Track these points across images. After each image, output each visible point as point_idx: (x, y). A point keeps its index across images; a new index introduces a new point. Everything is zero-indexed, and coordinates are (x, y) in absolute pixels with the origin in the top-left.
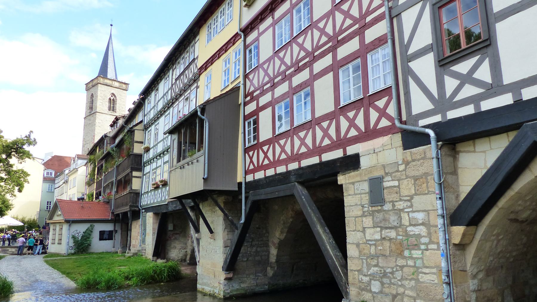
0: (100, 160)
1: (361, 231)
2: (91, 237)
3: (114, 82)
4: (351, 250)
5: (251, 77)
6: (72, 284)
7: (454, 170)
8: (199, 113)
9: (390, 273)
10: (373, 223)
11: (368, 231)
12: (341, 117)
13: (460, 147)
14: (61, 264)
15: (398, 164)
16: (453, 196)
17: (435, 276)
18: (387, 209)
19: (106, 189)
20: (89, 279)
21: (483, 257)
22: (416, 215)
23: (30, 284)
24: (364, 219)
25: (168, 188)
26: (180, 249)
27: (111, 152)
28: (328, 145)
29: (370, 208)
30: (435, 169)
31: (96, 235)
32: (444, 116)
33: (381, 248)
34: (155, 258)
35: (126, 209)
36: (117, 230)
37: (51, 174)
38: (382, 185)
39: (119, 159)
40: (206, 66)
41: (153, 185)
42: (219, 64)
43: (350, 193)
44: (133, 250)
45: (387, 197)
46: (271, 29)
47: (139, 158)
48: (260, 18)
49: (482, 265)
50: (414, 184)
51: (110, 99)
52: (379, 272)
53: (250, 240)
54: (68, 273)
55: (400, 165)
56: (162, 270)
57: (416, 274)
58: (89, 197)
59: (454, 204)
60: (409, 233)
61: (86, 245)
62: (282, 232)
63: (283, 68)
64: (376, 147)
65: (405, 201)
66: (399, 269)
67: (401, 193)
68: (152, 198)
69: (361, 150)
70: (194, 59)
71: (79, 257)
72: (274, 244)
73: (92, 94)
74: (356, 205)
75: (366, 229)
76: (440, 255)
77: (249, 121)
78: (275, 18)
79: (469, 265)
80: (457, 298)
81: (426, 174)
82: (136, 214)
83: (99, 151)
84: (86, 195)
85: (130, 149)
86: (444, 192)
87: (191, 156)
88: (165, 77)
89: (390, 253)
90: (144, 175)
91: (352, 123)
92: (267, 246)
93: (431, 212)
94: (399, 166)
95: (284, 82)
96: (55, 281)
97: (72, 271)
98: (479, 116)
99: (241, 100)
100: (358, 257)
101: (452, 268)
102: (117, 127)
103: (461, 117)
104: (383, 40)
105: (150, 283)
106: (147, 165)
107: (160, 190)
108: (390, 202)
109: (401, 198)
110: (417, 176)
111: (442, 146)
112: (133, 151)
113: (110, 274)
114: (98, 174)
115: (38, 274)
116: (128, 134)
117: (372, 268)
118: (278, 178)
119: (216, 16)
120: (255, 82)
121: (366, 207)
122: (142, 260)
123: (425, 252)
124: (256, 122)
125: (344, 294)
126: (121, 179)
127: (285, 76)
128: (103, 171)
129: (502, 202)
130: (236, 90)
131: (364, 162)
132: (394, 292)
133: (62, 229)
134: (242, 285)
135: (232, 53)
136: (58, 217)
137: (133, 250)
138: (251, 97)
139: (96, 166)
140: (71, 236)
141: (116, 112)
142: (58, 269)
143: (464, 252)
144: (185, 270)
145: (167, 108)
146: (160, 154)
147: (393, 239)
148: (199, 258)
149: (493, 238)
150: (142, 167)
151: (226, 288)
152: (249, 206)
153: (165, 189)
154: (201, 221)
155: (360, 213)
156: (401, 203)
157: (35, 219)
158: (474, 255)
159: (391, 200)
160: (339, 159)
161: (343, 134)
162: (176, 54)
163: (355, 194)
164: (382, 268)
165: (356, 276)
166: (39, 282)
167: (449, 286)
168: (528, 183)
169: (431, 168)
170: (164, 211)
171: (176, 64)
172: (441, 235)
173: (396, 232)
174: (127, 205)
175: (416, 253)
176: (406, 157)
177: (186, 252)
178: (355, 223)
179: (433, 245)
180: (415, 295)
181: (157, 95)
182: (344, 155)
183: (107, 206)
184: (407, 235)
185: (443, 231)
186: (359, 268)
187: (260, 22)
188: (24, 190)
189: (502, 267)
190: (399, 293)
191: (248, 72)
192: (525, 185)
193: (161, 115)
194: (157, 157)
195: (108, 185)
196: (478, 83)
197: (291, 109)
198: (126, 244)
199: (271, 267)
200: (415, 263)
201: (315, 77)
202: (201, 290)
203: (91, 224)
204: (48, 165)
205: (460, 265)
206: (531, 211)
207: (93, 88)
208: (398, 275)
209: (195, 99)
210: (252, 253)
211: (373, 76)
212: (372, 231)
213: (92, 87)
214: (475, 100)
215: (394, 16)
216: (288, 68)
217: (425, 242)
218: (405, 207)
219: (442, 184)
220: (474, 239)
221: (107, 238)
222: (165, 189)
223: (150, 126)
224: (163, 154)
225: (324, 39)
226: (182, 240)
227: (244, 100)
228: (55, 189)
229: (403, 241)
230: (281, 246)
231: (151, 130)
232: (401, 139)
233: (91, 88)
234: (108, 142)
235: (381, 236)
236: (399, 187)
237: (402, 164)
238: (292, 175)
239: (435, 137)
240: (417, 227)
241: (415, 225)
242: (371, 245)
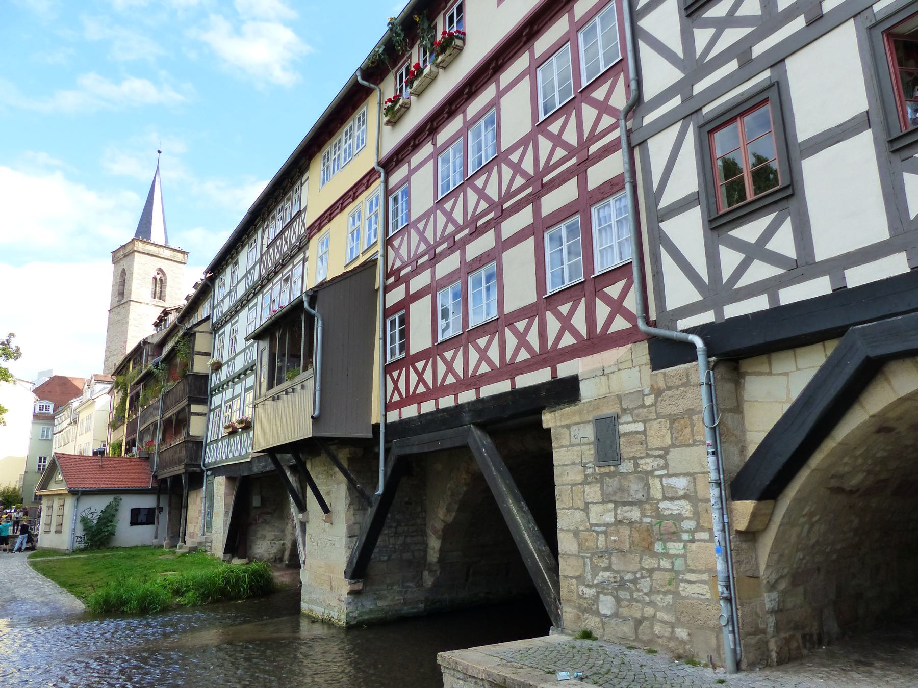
0: (134, 385)
1: (582, 510)
2: (116, 519)
4: (566, 543)
5: (396, 243)
6: (79, 606)
7: (736, 404)
8: (306, 305)
9: (631, 581)
10: (602, 495)
11: (593, 509)
12: (549, 314)
13: (746, 365)
15: (643, 394)
16: (735, 448)
17: (707, 587)
18: (624, 471)
19: (144, 436)
20: (108, 595)
21: (787, 552)
22: (673, 481)
24: (587, 488)
25: (252, 432)
26: (273, 540)
27: (154, 370)
28: (525, 361)
29: (597, 468)
30: (705, 404)
31: (124, 516)
32: (719, 313)
33: (616, 538)
34: (228, 556)
35: (179, 469)
36: (162, 508)
37: (48, 408)
38: (617, 430)
39: (168, 382)
41: (227, 427)
42: (342, 220)
43: (563, 444)
44: (190, 542)
45: (626, 449)
46: (431, 163)
47: (203, 381)
48: (412, 144)
49: (785, 568)
50: (671, 428)
51: (155, 278)
52: (612, 580)
53: (394, 525)
54: (72, 585)
55: (646, 395)
56: (240, 578)
57: (674, 583)
58: (114, 449)
59: (737, 462)
60: (662, 513)
61: (106, 534)
62: (448, 510)
63: (451, 228)
64: (606, 365)
65: (656, 457)
66: (646, 575)
67: (649, 444)
68: (225, 451)
69: (581, 370)
70: (300, 211)
72: (435, 532)
73: (124, 269)
74: (574, 463)
75: (589, 505)
76: (714, 551)
77: (392, 318)
78: (438, 145)
79: (763, 567)
80: (743, 624)
81: (690, 412)
82: (196, 479)
83: (134, 368)
84: (108, 446)
85: (186, 365)
86: (720, 443)
87: (291, 378)
88: (250, 243)
89: (630, 547)
90: (210, 410)
91: (566, 324)
92: (424, 534)
93: (700, 478)
94: (645, 398)
95: (453, 252)
96: (47, 599)
97: (79, 581)
98: (777, 313)
99: (379, 282)
100: (577, 553)
101: (735, 573)
103: (746, 316)
104: (617, 184)
105: (218, 601)
106: (216, 394)
107: (238, 437)
108: (630, 459)
109: (649, 452)
110: (675, 414)
111: (716, 364)
112: (192, 369)
113: (147, 585)
114: (130, 409)
115: (17, 587)
116: (183, 339)
117: (601, 574)
118: (441, 416)
119: (339, 138)
120: (404, 252)
121: (590, 468)
122: (205, 559)
123: (689, 544)
124: (404, 321)
125: (552, 619)
127: (454, 242)
128: (140, 403)
129: (817, 459)
130: (371, 264)
131: (586, 390)
132: (638, 615)
133: (63, 505)
134: (380, 604)
135: (364, 203)
136: (58, 486)
137: (190, 542)
138: (396, 277)
139: (127, 396)
140: (79, 519)
141: (164, 301)
142: (54, 578)
143: (755, 546)
144: (281, 577)
145: (252, 295)
146: (240, 375)
147: (636, 522)
148: (305, 556)
149: (802, 520)
151: (351, 608)
152: (391, 464)
153: (248, 436)
154: (309, 491)
155: (579, 478)
156: (648, 460)
157: (17, 488)
158: (771, 549)
159: (632, 455)
160: (544, 384)
161: (550, 343)
162: (269, 203)
163: (572, 445)
164: (617, 572)
165: (574, 588)
166: (18, 602)
167: (729, 605)
168: (858, 427)
169: (698, 401)
170: (246, 474)
171: (269, 220)
172: (715, 515)
173: (641, 510)
174: (179, 463)
175: (675, 548)
176: (657, 383)
177: (284, 544)
178: (571, 494)
179: (703, 533)
180: (673, 620)
181: (236, 272)
182: (552, 378)
183: (145, 465)
184: (659, 516)
185: (718, 509)
186: (578, 574)
187: (411, 151)
189: (819, 569)
190: (646, 615)
191: (390, 234)
192: (853, 431)
193: (243, 307)
194: (234, 379)
195: (147, 428)
196: (774, 259)
197: (465, 298)
198: (177, 532)
199: (431, 571)
200: (672, 563)
201: (504, 245)
202: (307, 612)
203: (116, 496)
204: (42, 392)
205: (748, 567)
206: (865, 474)
207: (125, 259)
208: (645, 585)
209: (301, 279)
210: (397, 547)
211: (601, 246)
212: (600, 508)
213: (124, 257)
214: (769, 287)
215: (636, 144)
216: (460, 229)
217: (689, 527)
218: (656, 468)
219: (717, 429)
220: (772, 523)
221: (144, 521)
222: (248, 436)
223: (222, 326)
224: (245, 374)
225: (519, 181)
226: (276, 525)
227: (384, 283)
229: (652, 527)
230: (447, 534)
231: (224, 333)
232: (647, 352)
233: (121, 259)
234: (150, 354)
235: (615, 518)
236: (644, 432)
237: (649, 395)
238: (465, 412)
239: (705, 348)
240: (675, 502)
241: (672, 499)
242: (598, 533)
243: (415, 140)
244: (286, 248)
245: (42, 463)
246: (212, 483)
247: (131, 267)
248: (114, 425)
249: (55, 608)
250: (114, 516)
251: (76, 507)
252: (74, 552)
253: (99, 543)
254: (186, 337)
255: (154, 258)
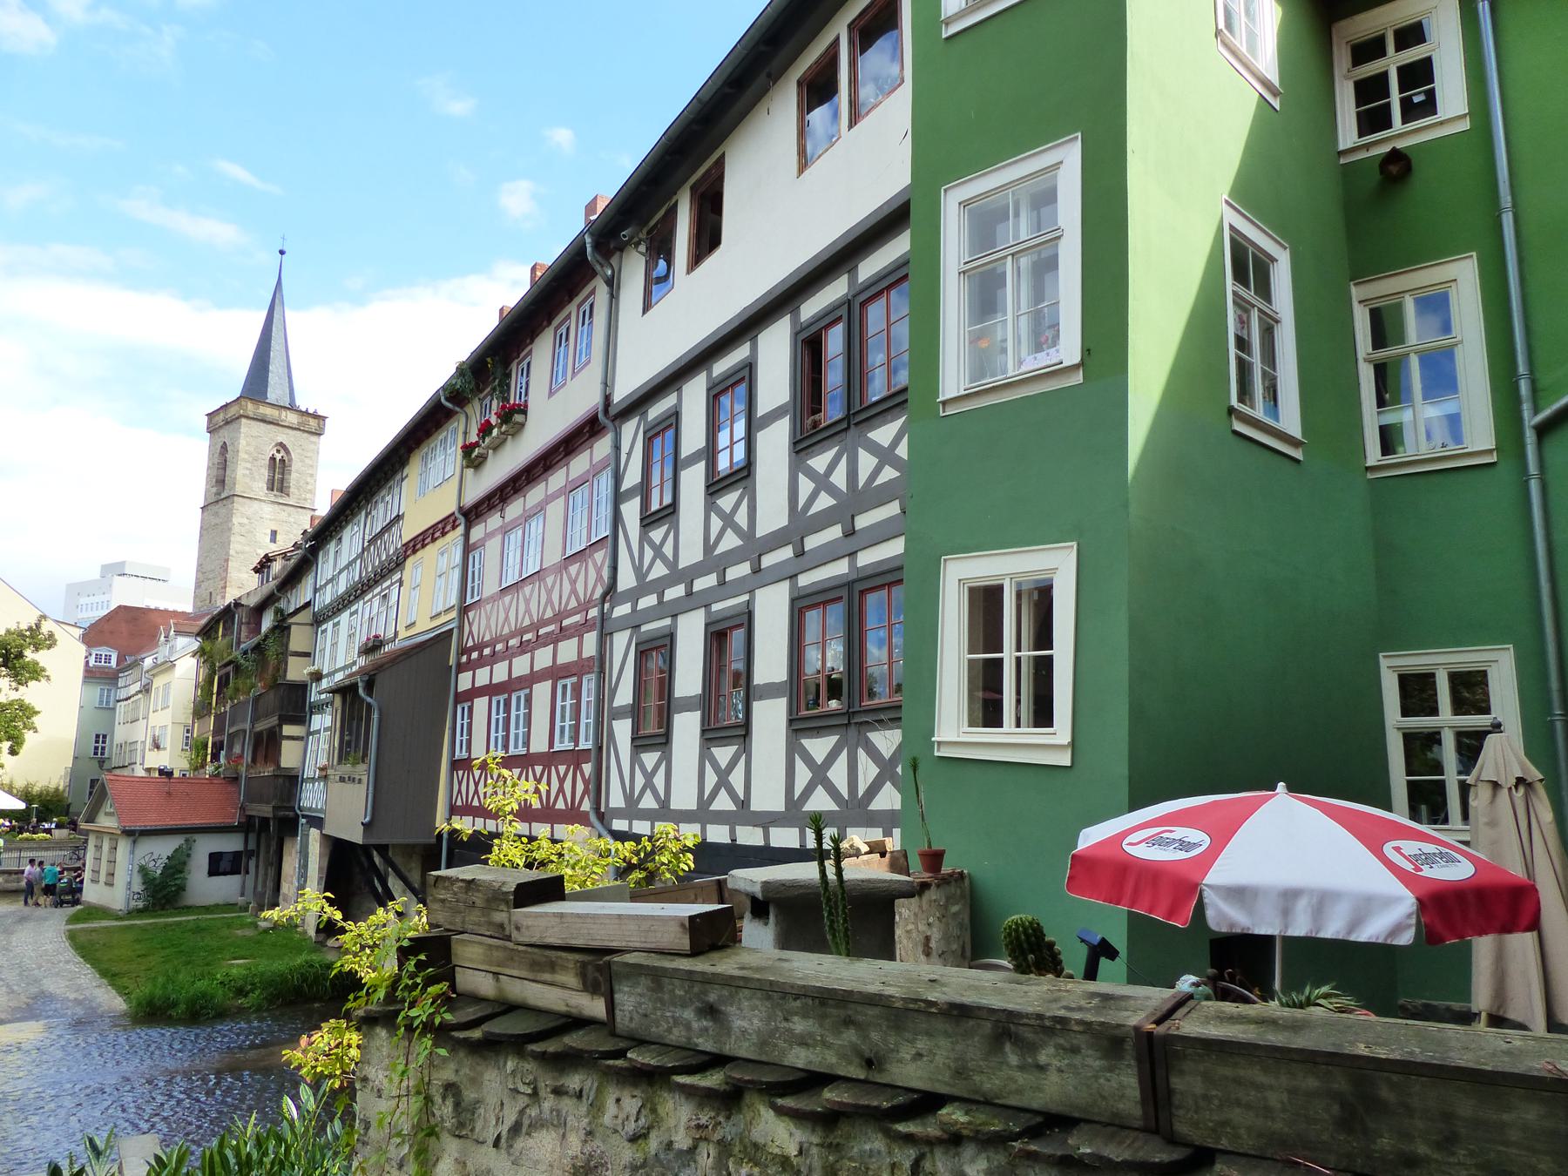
2: (187, 868)
3: (284, 413)
5: (471, 614)
6: (119, 1004)
8: (361, 691)
14: (104, 945)
23: (28, 1004)
27: (242, 661)
35: (266, 810)
37: (108, 659)
40: (414, 546)
42: (430, 552)
51: (273, 459)
54: (114, 975)
63: (506, 631)
70: (398, 516)
71: (151, 924)
78: (508, 519)
90: (309, 733)
102: (268, 581)
112: (285, 676)
114: (218, 693)
116: (274, 633)
126: (260, 733)
130: (443, 639)
140: (136, 868)
141: (288, 495)
150: (305, 712)
157: (61, 788)
183: (231, 788)
188: (23, 751)
191: (469, 601)
203: (188, 836)
204: (94, 635)
207: (227, 427)
221: (228, 869)
223: (325, 620)
228: (118, 701)
231: (325, 630)
243: (489, 500)
244: (384, 558)
245: (100, 744)
246: (308, 835)
247: (235, 440)
248: (200, 710)
249: (91, 1008)
250: (185, 863)
251: (132, 852)
252: (129, 913)
253: (163, 901)
254: (277, 631)
255: (272, 426)
